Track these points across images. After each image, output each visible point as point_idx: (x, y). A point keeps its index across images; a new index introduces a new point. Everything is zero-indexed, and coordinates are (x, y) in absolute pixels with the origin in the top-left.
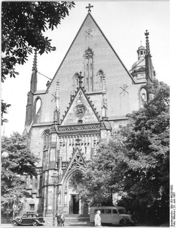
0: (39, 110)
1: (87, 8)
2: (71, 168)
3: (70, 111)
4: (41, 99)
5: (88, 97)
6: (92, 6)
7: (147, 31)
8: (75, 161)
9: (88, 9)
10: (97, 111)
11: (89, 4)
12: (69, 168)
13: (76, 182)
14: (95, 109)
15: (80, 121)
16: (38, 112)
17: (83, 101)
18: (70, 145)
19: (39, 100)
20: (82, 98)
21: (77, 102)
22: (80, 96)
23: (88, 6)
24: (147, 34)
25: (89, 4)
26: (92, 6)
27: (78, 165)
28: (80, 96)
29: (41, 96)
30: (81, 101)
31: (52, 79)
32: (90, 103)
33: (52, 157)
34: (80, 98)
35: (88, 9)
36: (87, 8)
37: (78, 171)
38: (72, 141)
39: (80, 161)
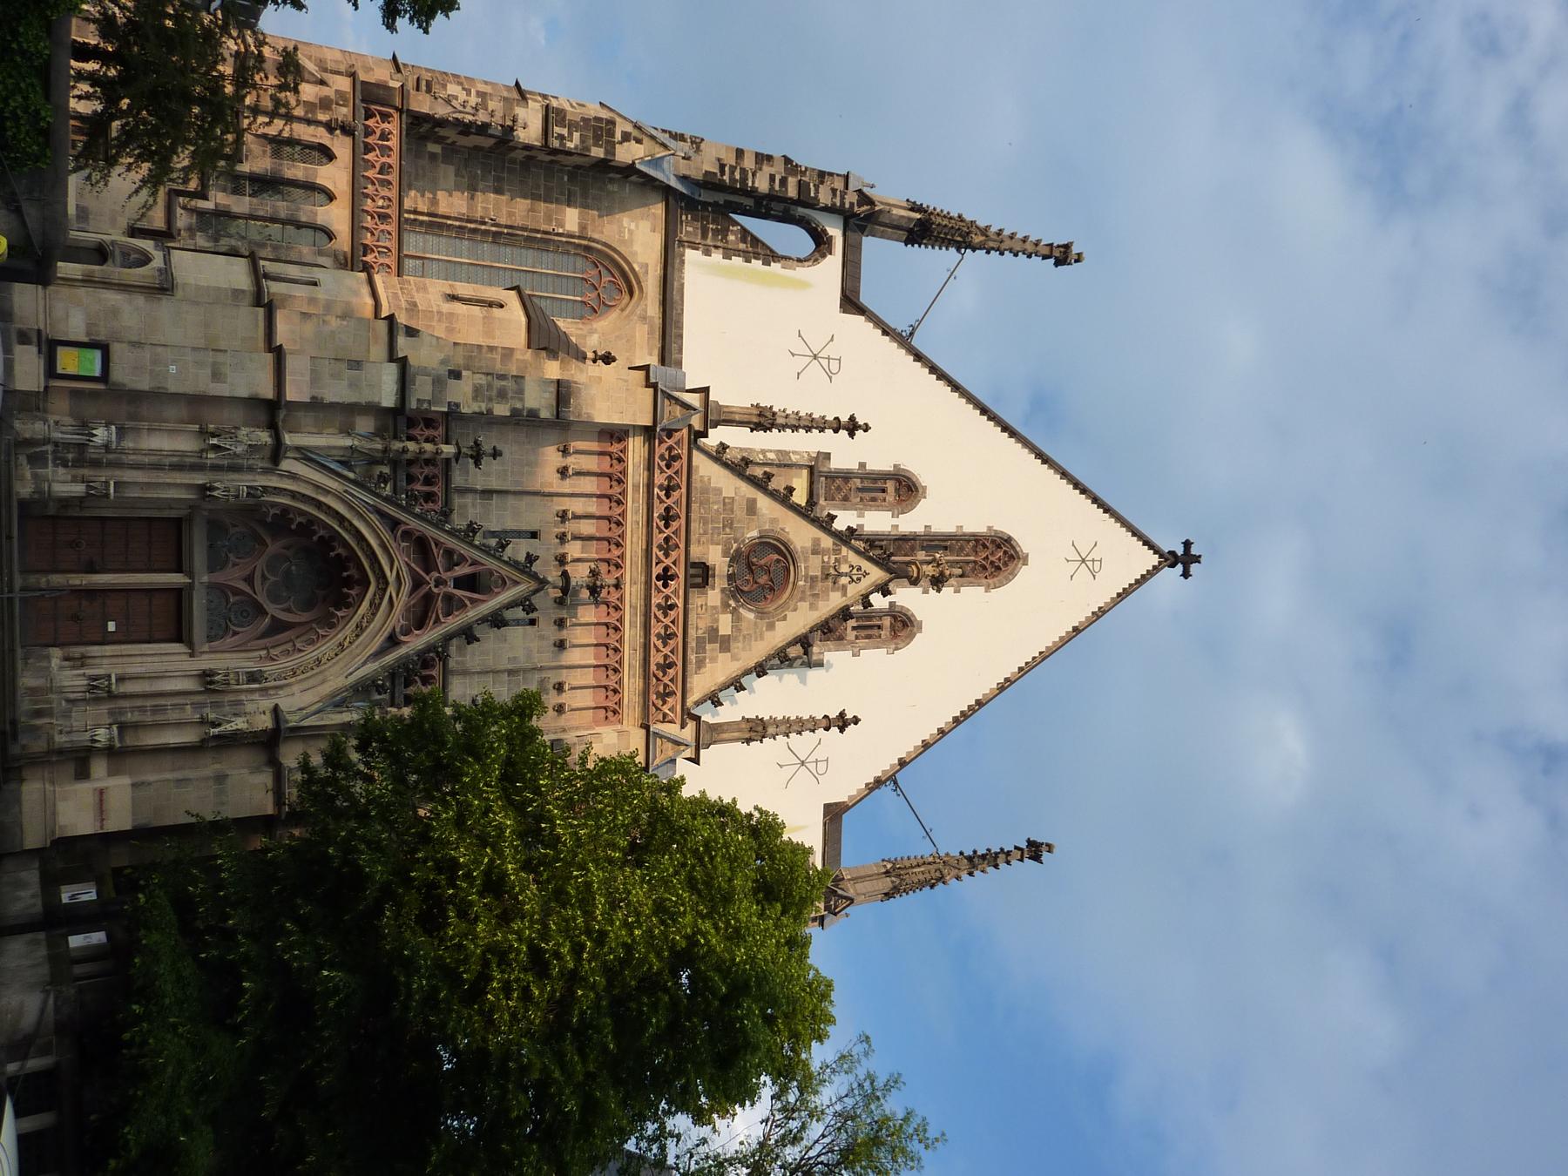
0: (756, 241)
1: (1187, 544)
2: (403, 527)
6: (1186, 574)
7: (1050, 848)
8: (452, 559)
9: (1180, 551)
11: (1197, 559)
12: (402, 516)
13: (287, 548)
16: (745, 233)
17: (812, 587)
18: (563, 516)
19: (808, 245)
20: (830, 584)
21: (816, 551)
22: (846, 575)
23: (1194, 551)
24: (1035, 851)
25: (1197, 559)
26: (1186, 574)
27: (418, 583)
28: (846, 575)
29: (832, 264)
30: (813, 579)
31: (915, 342)
33: (490, 386)
34: (831, 576)
35: (1180, 551)
36: (1187, 544)
37: (372, 579)
38: (587, 528)
39: (449, 598)
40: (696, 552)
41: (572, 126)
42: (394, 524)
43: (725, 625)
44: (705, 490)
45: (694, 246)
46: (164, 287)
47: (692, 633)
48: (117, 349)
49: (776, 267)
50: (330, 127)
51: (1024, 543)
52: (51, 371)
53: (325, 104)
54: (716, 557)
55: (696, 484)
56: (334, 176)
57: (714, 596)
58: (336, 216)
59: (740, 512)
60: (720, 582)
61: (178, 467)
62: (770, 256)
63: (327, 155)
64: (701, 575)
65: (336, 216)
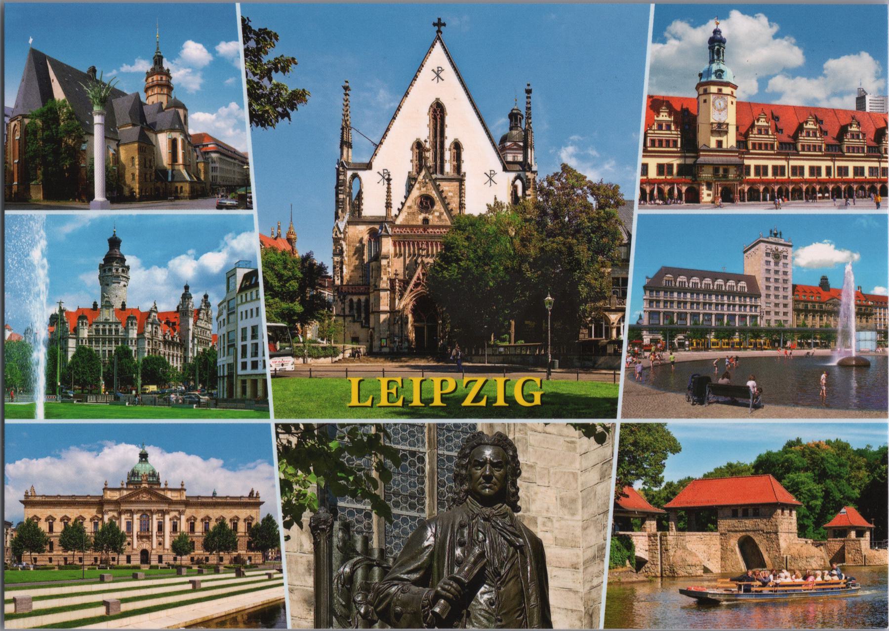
3: (408, 204)
4: (360, 179)
5: (438, 183)
10: (450, 207)
14: (449, 204)
15: (426, 220)
19: (356, 179)
29: (361, 173)
32: (440, 193)
40: (420, 223)
41: (336, 248)
42: (411, 291)
43: (437, 214)
44: (406, 220)
45: (360, 214)
46: (373, 329)
47: (439, 223)
48: (382, 337)
49: (363, 190)
50: (345, 299)
51: (431, 100)
52: (386, 346)
53: (341, 300)
54: (421, 217)
55: (405, 223)
56: (355, 299)
57: (430, 217)
58: (363, 298)
59: (411, 211)
60: (427, 215)
61: (402, 327)
62: (360, 193)
63: (351, 301)
64: (426, 220)
65: (363, 298)
